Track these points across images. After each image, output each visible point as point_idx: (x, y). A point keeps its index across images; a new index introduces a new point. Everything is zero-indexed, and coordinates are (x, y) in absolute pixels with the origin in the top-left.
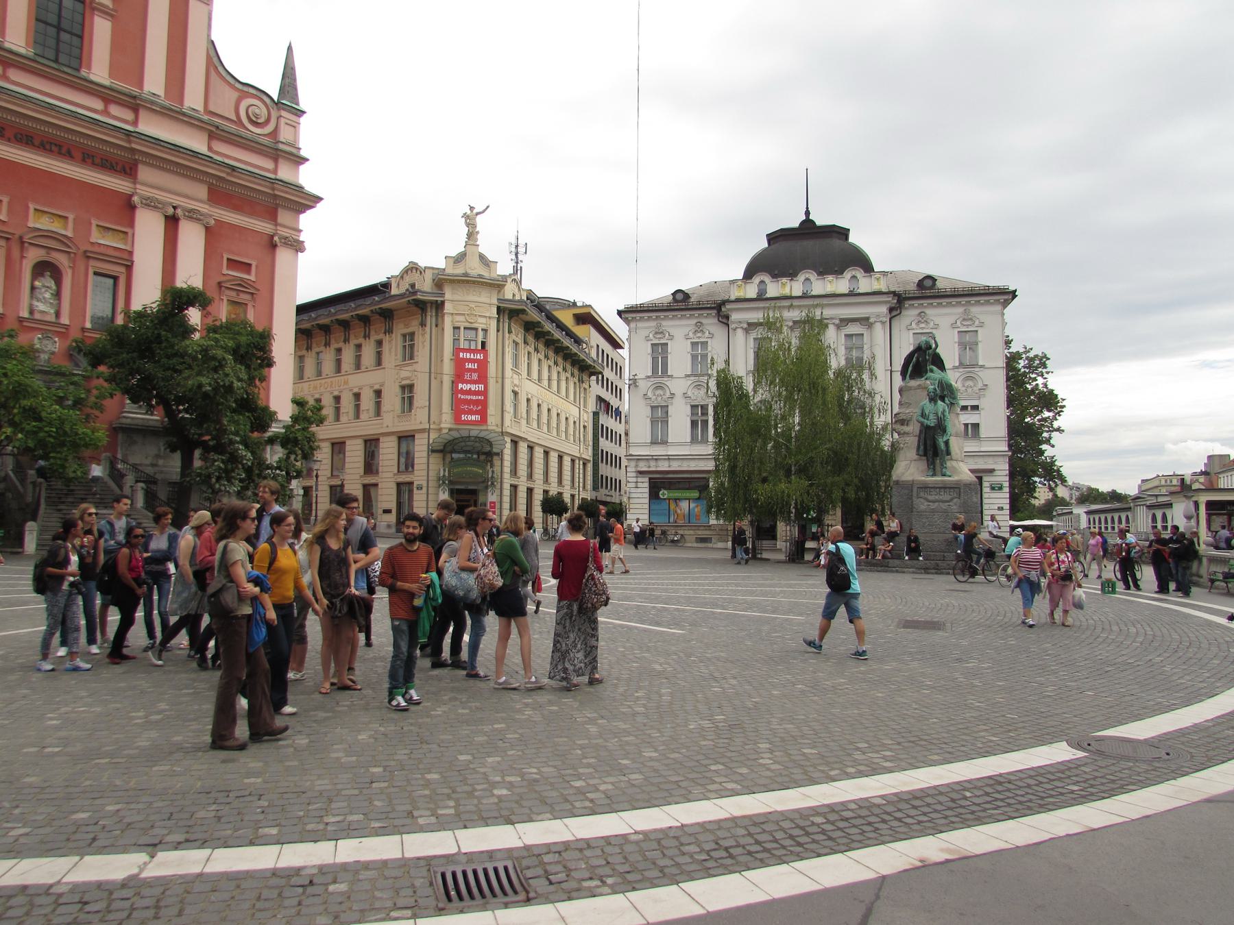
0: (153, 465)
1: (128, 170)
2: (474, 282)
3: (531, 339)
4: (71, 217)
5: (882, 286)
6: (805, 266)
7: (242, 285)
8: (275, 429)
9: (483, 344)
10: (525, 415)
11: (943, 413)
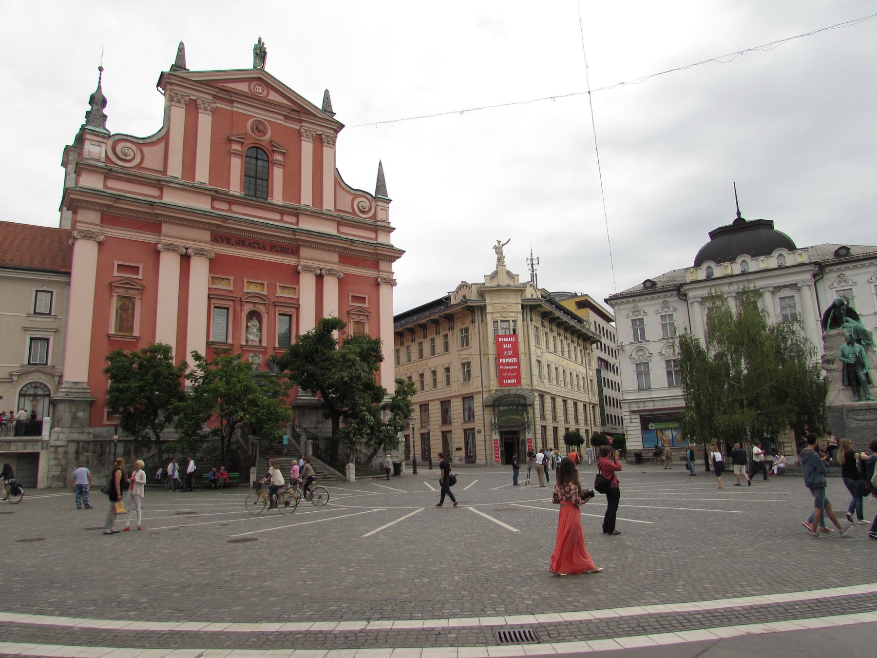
0: (316, 428)
1: (294, 251)
2: (504, 290)
3: (546, 323)
4: (266, 283)
5: (804, 259)
6: (742, 252)
7: (361, 310)
8: (386, 400)
9: (514, 330)
10: (547, 376)
11: (860, 352)
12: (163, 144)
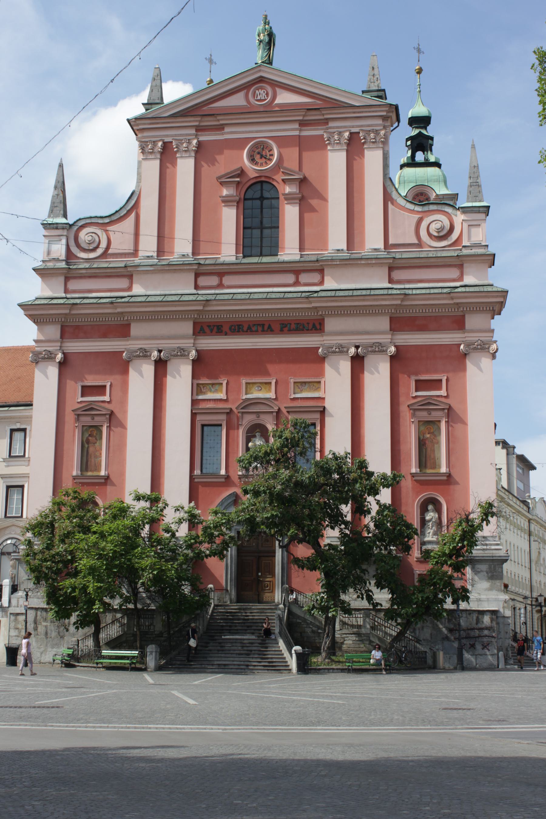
12: (133, 215)
